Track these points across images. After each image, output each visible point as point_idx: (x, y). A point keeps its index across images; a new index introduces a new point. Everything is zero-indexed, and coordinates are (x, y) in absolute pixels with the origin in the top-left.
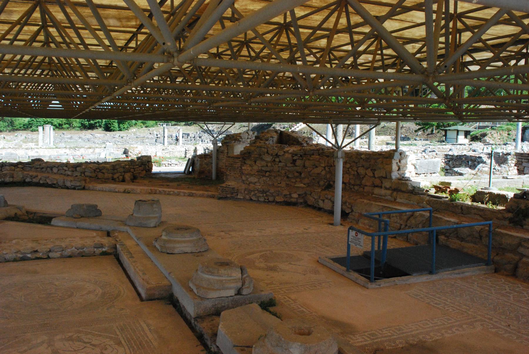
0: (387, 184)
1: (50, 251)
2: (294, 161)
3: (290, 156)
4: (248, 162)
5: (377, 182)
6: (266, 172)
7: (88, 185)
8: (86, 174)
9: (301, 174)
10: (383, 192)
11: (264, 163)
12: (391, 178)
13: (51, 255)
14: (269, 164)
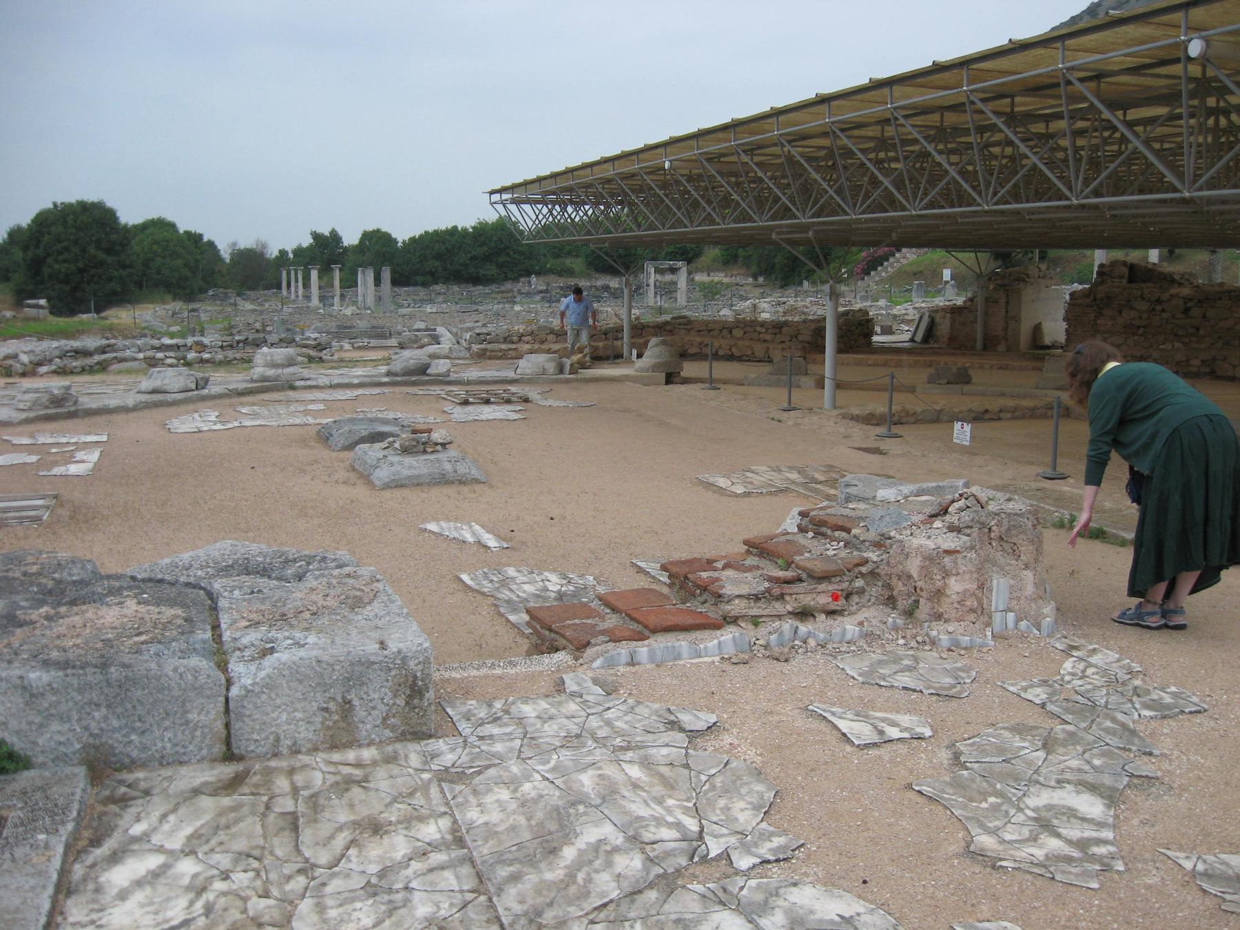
1: (1001, 411)
2: (1187, 311)
3: (1181, 302)
6: (1139, 327)
8: (801, 338)
9: (1198, 329)
11: (1133, 314)
13: (1001, 415)
14: (1145, 316)
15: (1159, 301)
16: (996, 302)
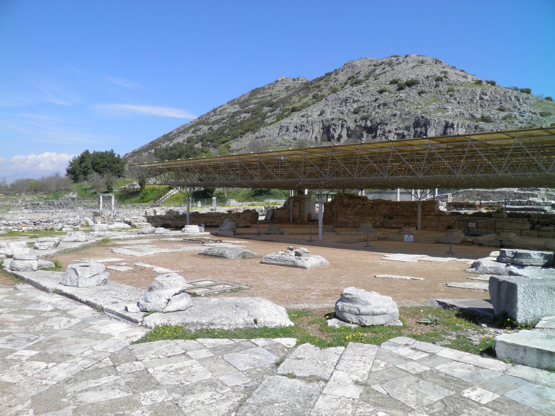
0: (434, 214)
2: (372, 208)
4: (349, 208)
5: (427, 213)
7: (252, 225)
10: (430, 217)
11: (357, 209)
12: (435, 211)
15: (364, 205)
16: (296, 206)
